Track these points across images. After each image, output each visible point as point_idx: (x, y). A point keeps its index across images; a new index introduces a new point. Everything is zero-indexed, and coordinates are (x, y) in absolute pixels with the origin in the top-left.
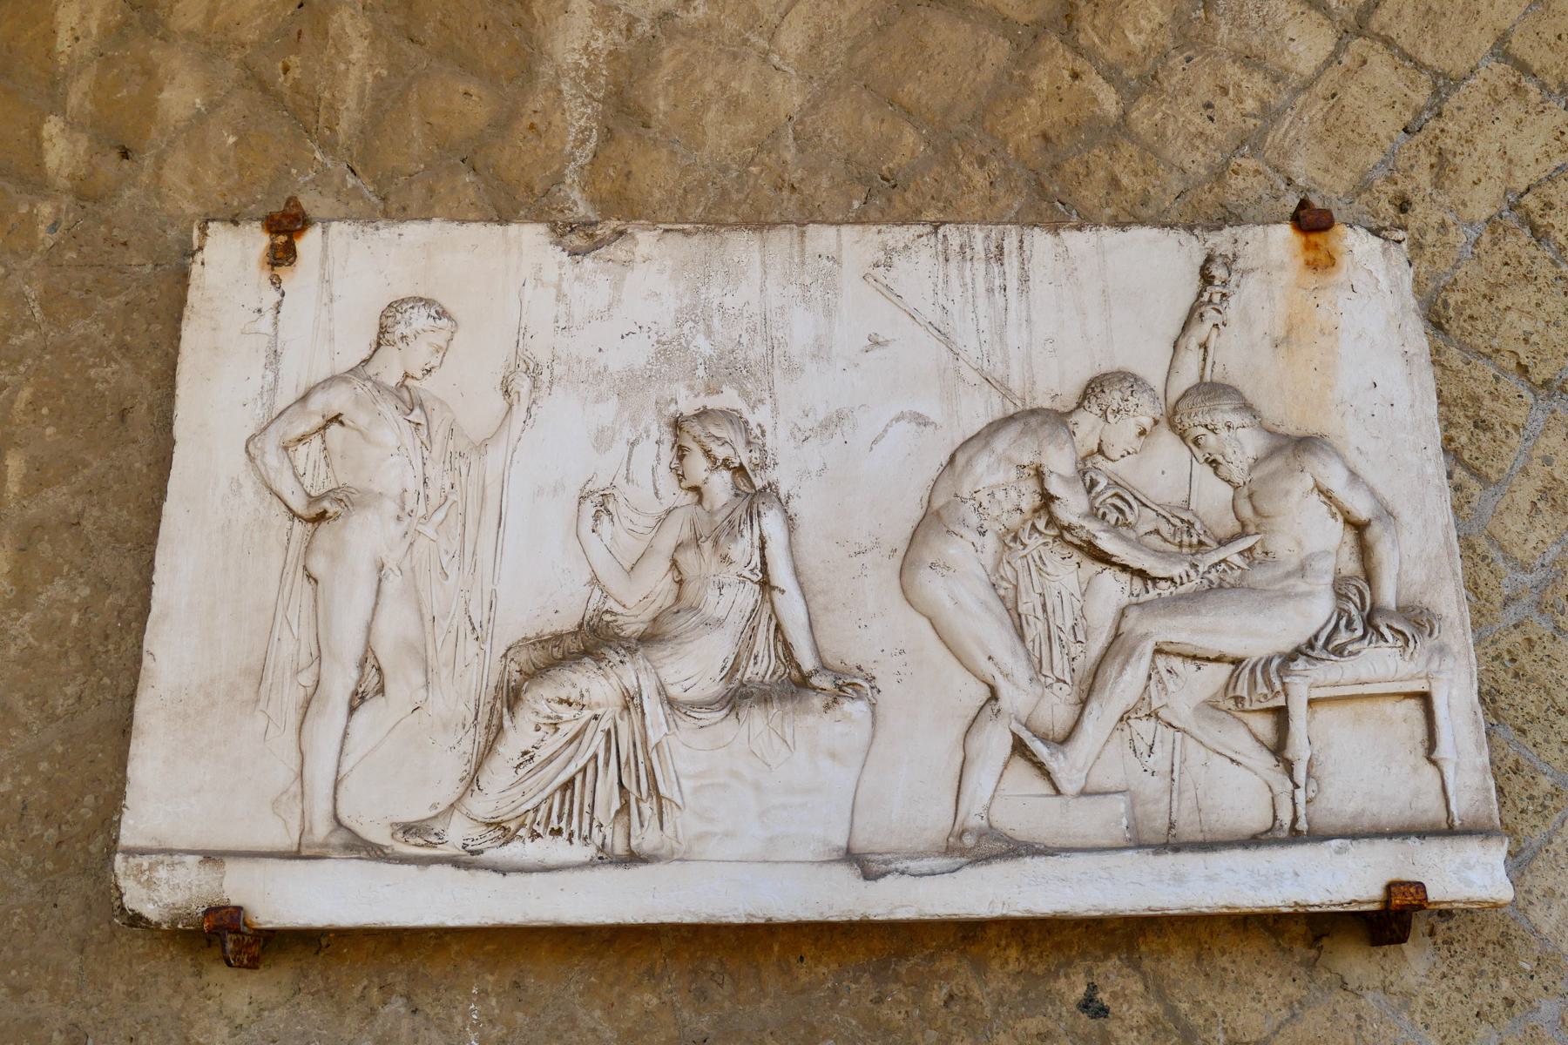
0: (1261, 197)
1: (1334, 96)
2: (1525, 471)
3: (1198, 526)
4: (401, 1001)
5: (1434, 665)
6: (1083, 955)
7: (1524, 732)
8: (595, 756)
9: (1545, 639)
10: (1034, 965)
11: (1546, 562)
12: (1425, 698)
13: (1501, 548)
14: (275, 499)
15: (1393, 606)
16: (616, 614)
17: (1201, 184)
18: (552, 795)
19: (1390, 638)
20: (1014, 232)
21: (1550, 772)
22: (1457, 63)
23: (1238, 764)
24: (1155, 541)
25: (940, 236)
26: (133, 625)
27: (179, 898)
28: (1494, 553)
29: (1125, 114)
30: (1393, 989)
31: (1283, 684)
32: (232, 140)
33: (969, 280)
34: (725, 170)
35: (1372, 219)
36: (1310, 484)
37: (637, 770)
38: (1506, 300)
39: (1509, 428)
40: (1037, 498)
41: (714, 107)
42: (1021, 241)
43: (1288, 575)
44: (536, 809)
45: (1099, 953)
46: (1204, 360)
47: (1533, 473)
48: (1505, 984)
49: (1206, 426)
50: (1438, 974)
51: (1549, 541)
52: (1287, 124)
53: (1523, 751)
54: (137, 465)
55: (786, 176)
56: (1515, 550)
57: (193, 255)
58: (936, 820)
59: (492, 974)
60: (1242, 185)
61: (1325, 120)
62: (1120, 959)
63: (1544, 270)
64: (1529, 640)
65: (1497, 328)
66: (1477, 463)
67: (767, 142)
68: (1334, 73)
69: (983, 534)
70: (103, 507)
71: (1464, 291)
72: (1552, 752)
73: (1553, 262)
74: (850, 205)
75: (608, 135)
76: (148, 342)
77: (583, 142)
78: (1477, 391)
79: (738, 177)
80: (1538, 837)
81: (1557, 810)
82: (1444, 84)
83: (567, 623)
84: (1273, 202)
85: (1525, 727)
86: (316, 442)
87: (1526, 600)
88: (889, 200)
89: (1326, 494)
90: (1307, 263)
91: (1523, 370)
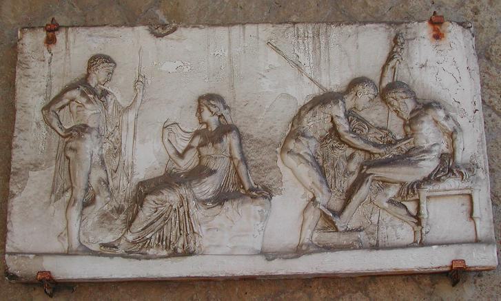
12: (470, 196)
45: (354, 291)
55: (238, 4)
57: (19, 41)
60: (415, 4)
74: (263, 14)
88: (278, 12)
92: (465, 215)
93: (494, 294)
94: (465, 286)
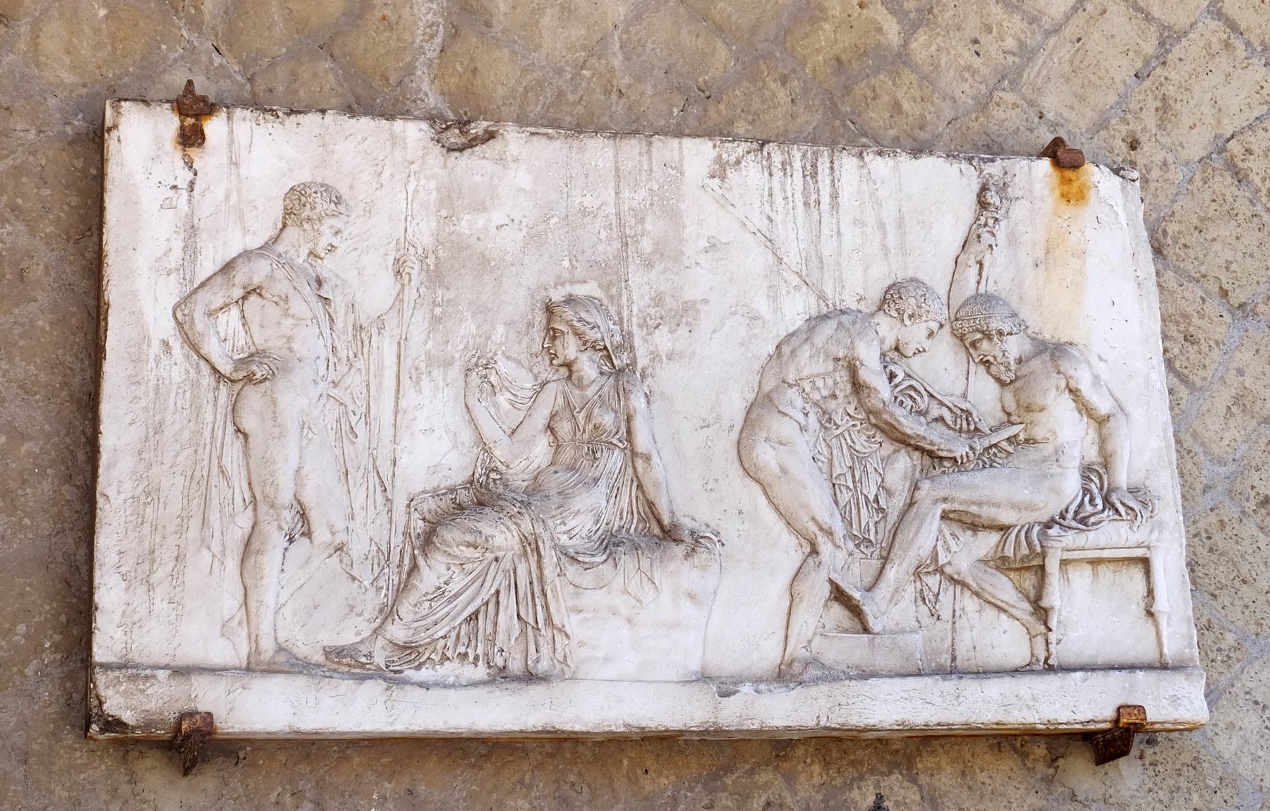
0: (1018, 129)
1: (1079, 40)
2: (1222, 380)
3: (975, 414)
4: (311, 806)
5: (1155, 535)
6: (873, 771)
7: (1214, 596)
8: (498, 592)
9: (1234, 521)
10: (833, 779)
11: (1237, 457)
12: (1145, 562)
13: (1203, 444)
14: (202, 363)
15: (1125, 488)
16: (501, 474)
17: (968, 113)
18: (461, 624)
19: (1123, 513)
20: (826, 154)
21: (1234, 630)
22: (1180, 19)
23: (1005, 611)
24: (940, 427)
25: (765, 153)
26: (48, 471)
27: (152, 706)
28: (1197, 448)
29: (905, 45)
30: (1111, 801)
31: (1042, 546)
32: (103, 12)
33: (790, 195)
34: (560, 72)
35: (1108, 154)
36: (1063, 384)
37: (535, 605)
38: (1212, 232)
39: (1212, 343)
40: (849, 386)
41: (549, 12)
42: (832, 162)
43: (1045, 460)
44: (444, 637)
45: (885, 769)
46: (980, 274)
47: (1229, 382)
48: (1195, 797)
49: (983, 332)
50: (1146, 788)
51: (1239, 440)
52: (1040, 63)
53: (1214, 612)
54: (40, 323)
55: (615, 82)
56: (1214, 446)
58: (768, 654)
59: (390, 782)
60: (1003, 116)
61: (1072, 62)
62: (901, 774)
63: (1243, 208)
64: (1221, 521)
65: (1205, 255)
66: (1186, 372)
67: (597, 48)
68: (1080, 19)
69: (806, 415)
70: (10, 360)
71: (1180, 222)
72: (1236, 614)
73: (1251, 202)
74: (671, 112)
75: (455, 33)
76: (40, 206)
77: (432, 36)
78: (1187, 309)
79: (572, 79)
80: (1223, 681)
81: (1238, 660)
82: (1169, 37)
83: (459, 477)
84: (1028, 133)
85: (1216, 592)
86: (234, 312)
87: (1220, 488)
88: (705, 110)
89: (1074, 392)
90: (1063, 195)
91: (1224, 293)
92: (1137, 609)
93: (1183, 783)
94: (1122, 762)
